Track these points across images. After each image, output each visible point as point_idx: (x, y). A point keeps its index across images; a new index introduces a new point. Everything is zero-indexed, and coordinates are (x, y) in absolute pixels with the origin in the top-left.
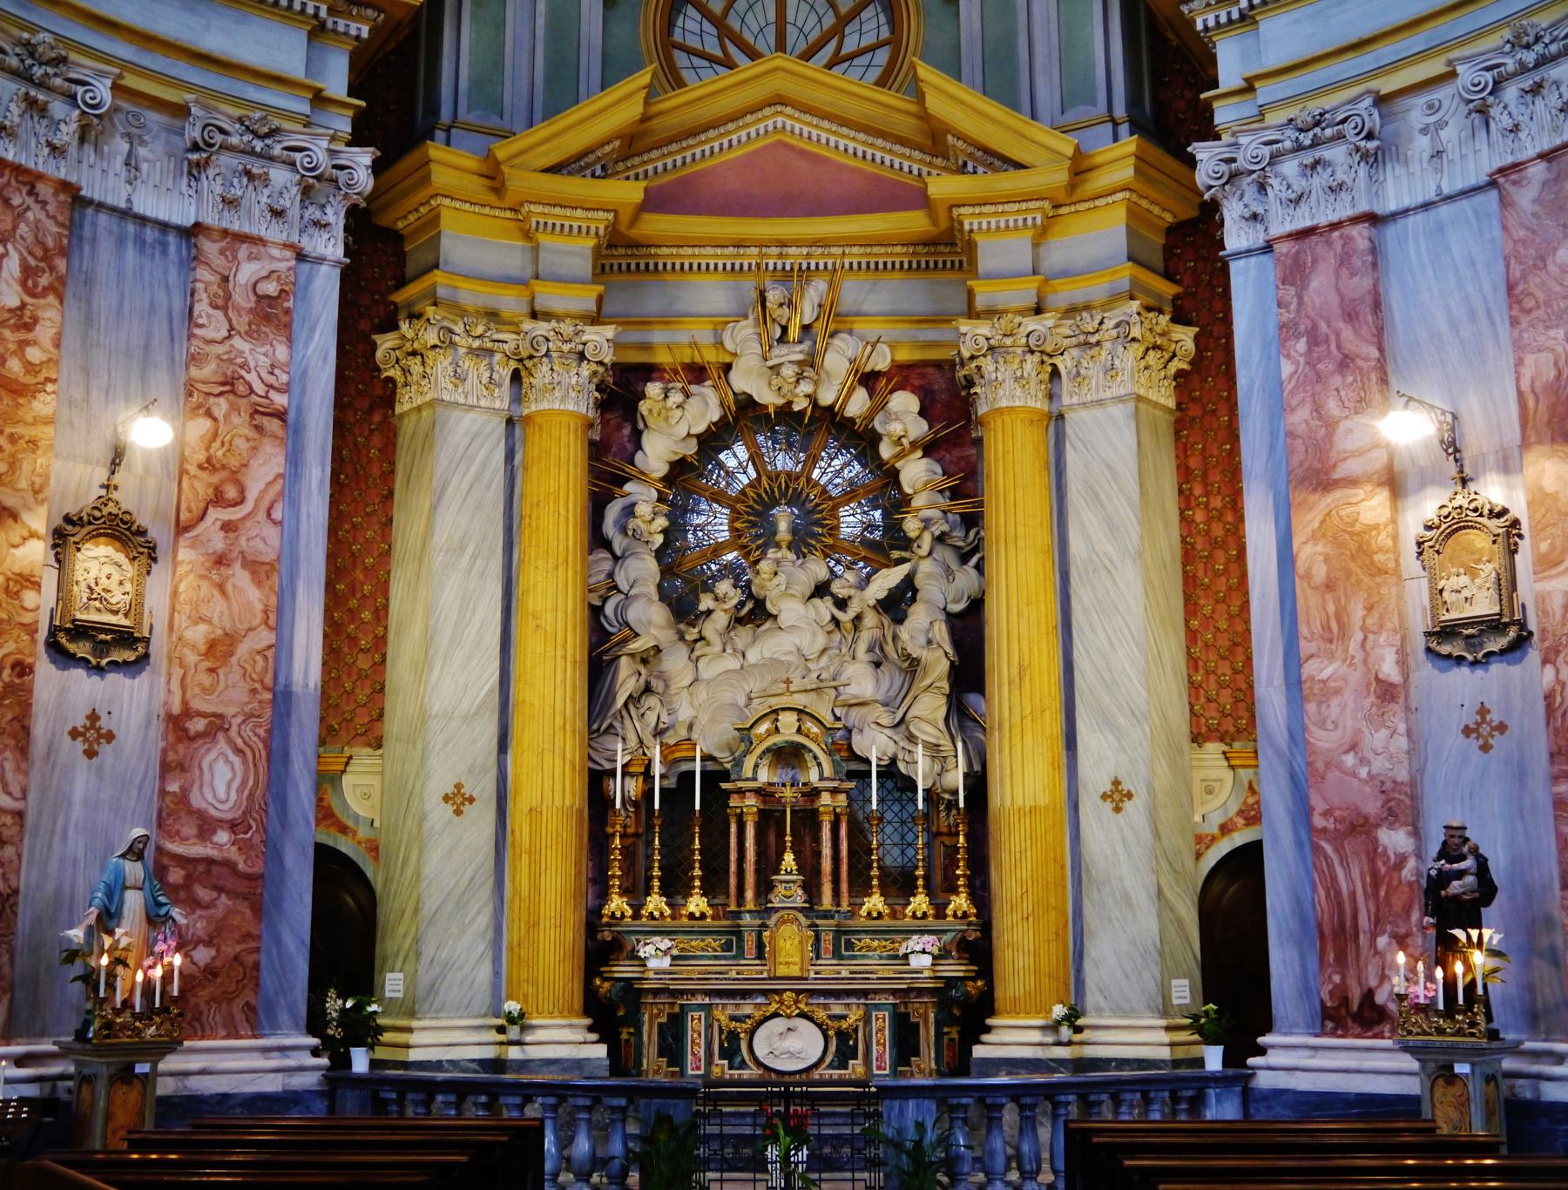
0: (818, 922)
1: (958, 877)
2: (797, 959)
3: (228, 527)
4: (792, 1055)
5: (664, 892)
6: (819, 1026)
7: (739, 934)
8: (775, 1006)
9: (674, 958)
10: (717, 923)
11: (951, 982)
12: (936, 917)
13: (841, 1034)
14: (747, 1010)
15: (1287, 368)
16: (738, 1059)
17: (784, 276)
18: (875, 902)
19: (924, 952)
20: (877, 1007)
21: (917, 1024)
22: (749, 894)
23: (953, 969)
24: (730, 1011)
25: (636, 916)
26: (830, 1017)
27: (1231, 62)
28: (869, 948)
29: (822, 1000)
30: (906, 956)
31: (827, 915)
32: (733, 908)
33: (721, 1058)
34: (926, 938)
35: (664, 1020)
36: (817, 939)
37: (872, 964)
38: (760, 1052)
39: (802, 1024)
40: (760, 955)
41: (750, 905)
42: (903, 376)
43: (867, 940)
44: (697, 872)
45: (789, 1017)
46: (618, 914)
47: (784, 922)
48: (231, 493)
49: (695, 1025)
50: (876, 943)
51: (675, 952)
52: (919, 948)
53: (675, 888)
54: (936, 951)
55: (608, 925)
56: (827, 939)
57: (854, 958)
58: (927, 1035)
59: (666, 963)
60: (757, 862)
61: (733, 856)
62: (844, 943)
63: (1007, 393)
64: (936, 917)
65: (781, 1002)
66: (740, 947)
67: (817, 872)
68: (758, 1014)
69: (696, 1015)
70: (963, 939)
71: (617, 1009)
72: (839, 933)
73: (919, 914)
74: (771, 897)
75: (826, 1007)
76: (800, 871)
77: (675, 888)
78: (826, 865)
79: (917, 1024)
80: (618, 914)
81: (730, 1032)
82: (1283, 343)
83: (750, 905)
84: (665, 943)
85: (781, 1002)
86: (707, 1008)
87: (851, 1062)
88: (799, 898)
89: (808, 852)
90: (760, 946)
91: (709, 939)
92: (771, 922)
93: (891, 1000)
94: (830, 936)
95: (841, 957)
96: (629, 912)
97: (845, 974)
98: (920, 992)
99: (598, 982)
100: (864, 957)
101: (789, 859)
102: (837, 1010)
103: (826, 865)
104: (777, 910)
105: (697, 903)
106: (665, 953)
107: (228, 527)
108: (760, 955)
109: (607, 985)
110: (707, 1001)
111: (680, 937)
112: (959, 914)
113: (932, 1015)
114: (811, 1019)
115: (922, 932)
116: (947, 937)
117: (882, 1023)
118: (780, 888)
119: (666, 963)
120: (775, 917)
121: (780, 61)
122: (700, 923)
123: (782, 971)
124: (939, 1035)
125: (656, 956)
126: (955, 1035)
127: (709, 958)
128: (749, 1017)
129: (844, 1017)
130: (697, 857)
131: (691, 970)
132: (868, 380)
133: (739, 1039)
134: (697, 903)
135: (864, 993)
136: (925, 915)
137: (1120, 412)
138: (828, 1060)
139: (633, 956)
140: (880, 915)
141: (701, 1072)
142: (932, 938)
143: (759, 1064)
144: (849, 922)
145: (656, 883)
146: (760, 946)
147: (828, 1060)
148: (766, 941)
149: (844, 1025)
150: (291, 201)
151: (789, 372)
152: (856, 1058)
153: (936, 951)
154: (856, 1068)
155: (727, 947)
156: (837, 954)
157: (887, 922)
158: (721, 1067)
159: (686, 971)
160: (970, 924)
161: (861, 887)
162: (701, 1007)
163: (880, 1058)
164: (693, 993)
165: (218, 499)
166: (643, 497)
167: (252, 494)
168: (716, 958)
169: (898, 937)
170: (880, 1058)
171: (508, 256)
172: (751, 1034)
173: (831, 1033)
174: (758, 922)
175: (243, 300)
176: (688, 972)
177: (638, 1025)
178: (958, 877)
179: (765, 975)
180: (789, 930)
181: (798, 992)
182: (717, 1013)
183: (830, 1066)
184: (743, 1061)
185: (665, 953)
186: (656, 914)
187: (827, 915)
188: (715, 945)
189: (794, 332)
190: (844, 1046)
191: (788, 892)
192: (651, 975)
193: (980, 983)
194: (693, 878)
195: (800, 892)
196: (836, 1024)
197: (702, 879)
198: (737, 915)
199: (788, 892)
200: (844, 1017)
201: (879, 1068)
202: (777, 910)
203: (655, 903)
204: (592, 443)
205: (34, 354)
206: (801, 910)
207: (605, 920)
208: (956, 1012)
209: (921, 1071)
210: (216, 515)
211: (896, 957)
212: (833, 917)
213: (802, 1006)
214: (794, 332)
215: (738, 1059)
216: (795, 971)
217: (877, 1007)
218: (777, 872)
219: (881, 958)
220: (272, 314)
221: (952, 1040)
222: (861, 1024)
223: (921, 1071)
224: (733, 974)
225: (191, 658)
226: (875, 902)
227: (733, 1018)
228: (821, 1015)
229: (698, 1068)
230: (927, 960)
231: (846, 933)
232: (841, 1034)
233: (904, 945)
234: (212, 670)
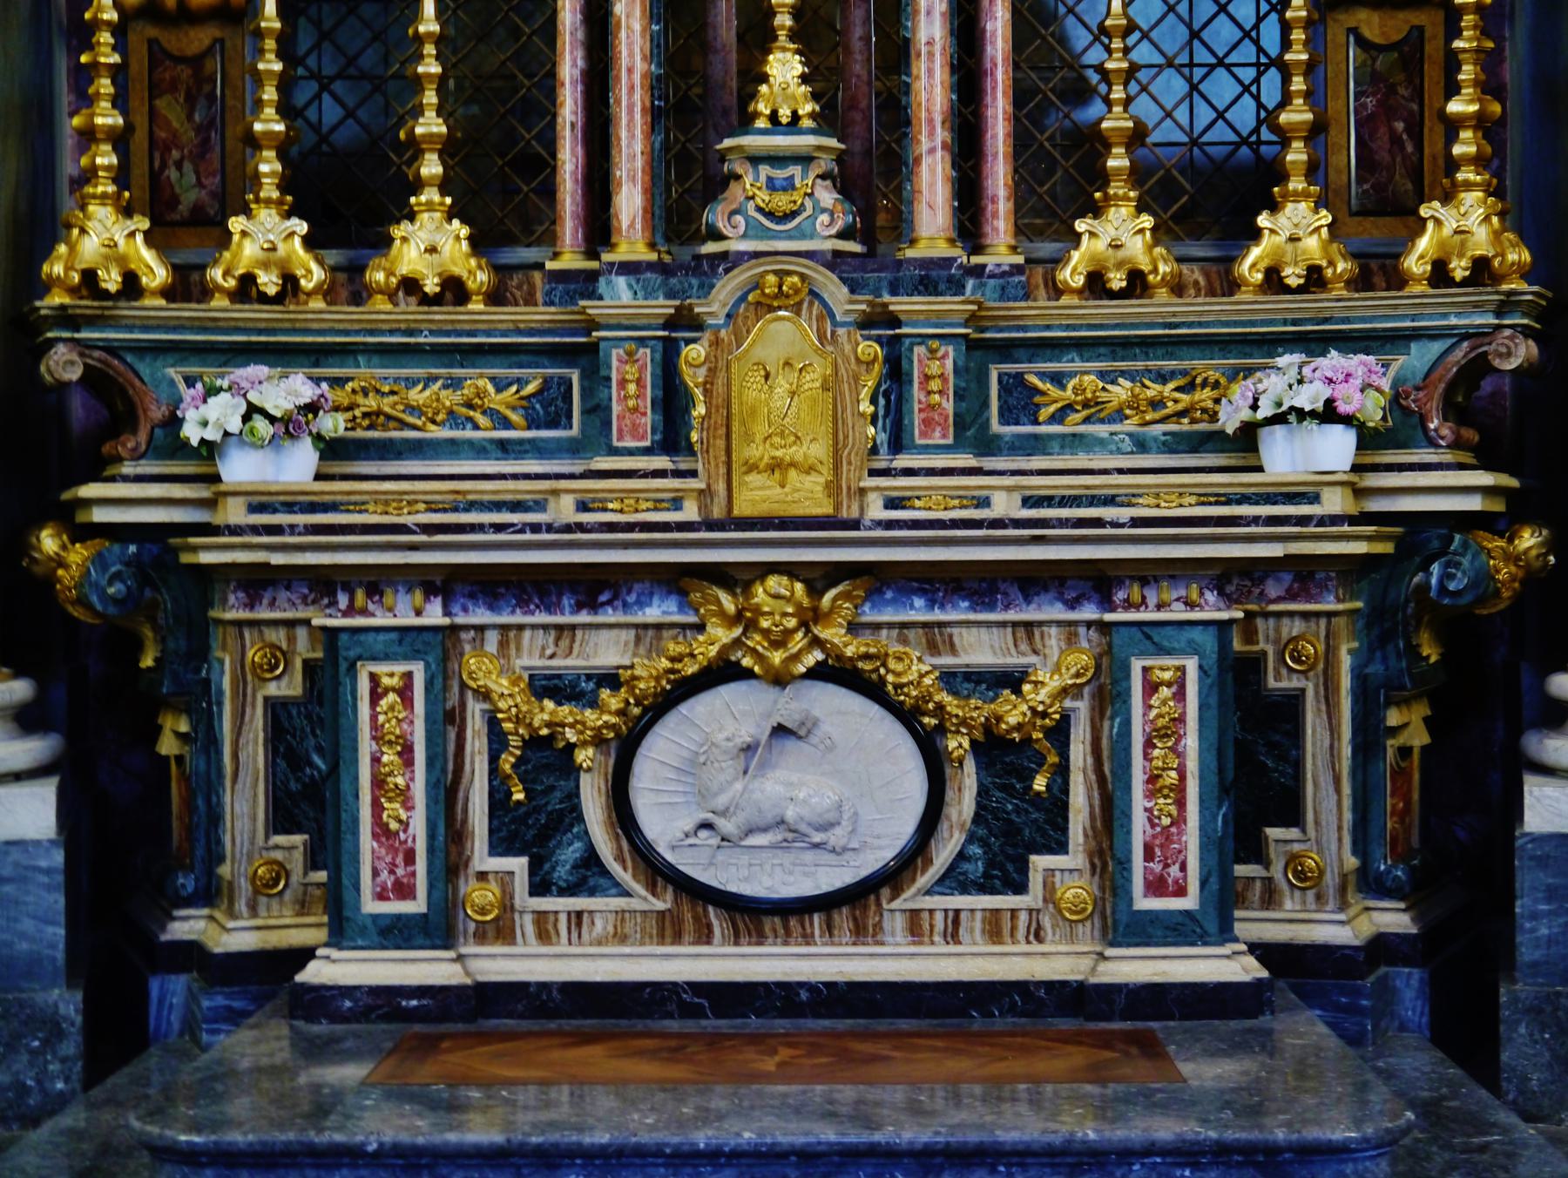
0: (901, 304)
1: (1452, 127)
2: (818, 450)
4: (793, 836)
5: (301, 195)
6: (907, 716)
7: (588, 357)
8: (721, 635)
9: (331, 449)
10: (505, 315)
11: (1421, 535)
12: (1361, 282)
13: (993, 748)
14: (605, 649)
16: (570, 853)
18: (1119, 233)
19: (1329, 414)
20: (1151, 636)
21: (1292, 704)
22: (629, 202)
23: (1449, 486)
24: (533, 655)
25: (187, 284)
26: (949, 679)
28: (1094, 409)
29: (918, 611)
30: (1247, 438)
31: (932, 278)
32: (571, 260)
33: (500, 846)
34: (1334, 361)
35: (290, 687)
36: (896, 372)
37: (1108, 467)
38: (663, 821)
39: (836, 707)
40: (672, 438)
41: (632, 243)
43: (1085, 377)
44: (431, 125)
45: (780, 680)
46: (111, 280)
47: (765, 307)
49: (386, 715)
50: (1121, 391)
51: (332, 424)
52: (1309, 397)
53: (349, 203)
54: (1372, 409)
55: (64, 318)
56: (935, 372)
57: (1035, 445)
58: (1325, 746)
59: (297, 466)
60: (656, 85)
61: (570, 66)
62: (1001, 385)
64: (1361, 282)
65: (746, 620)
66: (598, 412)
67: (896, 112)
68: (649, 671)
69: (390, 672)
70: (1478, 367)
71: (138, 648)
72: (979, 349)
73: (1293, 276)
74: (716, 215)
75: (935, 637)
76: (827, 120)
77: (349, 203)
78: (931, 88)
79: (1297, 697)
80: (111, 280)
81: (534, 743)
83: (632, 243)
84: (286, 391)
85: (746, 620)
86: (440, 647)
87: (1040, 862)
88: (825, 216)
89: (860, 66)
90: (672, 400)
91: (478, 380)
92: (715, 304)
93: (1213, 610)
94: (947, 360)
95: (988, 445)
96: (155, 272)
97: (1004, 505)
98: (1305, 574)
99: (48, 542)
100: (1075, 442)
101: (784, 67)
102: (981, 648)
103: (931, 88)
104: (729, 261)
105: (429, 243)
106: (289, 426)
108: (672, 438)
109: (78, 555)
110: (434, 615)
111: (364, 372)
112: (1459, 269)
113: (1346, 662)
114: (873, 690)
115: (1314, 343)
116: (1419, 357)
117: (1173, 702)
118: (752, 184)
119: (297, 466)
120: (726, 288)
122: (440, 314)
123: (756, 495)
124: (1369, 736)
125: (252, 439)
126: (1418, 738)
127: (479, 450)
128: (611, 680)
129: (1013, 680)
130: (430, 67)
131: (396, 493)
133: (571, 771)
134: (429, 243)
135: (1099, 581)
136: (1315, 278)
138: (944, 852)
139: (168, 439)
140: (1137, 283)
141: (416, 906)
142: (1357, 363)
143: (656, 870)
144: (1020, 308)
145: (269, 166)
146: (672, 400)
147: (944, 852)
148: (693, 378)
149: (1013, 712)
152: (1061, 847)
153: (1372, 409)
154: (1063, 871)
155: (548, 408)
156: (970, 431)
157: (1161, 304)
158: (496, 871)
159: (380, 492)
160: (1505, 306)
161: (1062, 184)
162: (409, 640)
163: (1163, 844)
164: (376, 582)
168: (505, 449)
169: (1207, 366)
170: (1163, 844)
172: (625, 748)
173: (956, 743)
174: (663, 306)
176: (385, 501)
177: (199, 701)
178: (1452, 127)
179: (690, 512)
180: (781, 335)
181: (819, 578)
182: (480, 667)
183: (954, 880)
184: (590, 859)
185: (289, 426)
186: (269, 282)
187: (932, 278)
188: (499, 400)
190: (1009, 806)
191: (783, 203)
192: (234, 513)
193: (1528, 540)
194: (415, 149)
195: (827, 196)
196: (976, 709)
197: (448, 149)
198: (584, 284)
199: (783, 203)
200: (1013, 680)
201: (1157, 886)
202: (729, 261)
203: (266, 238)
206: (835, 261)
207: (57, 298)
208: (1430, 651)
209: (1305, 879)
211: (1213, 440)
212: (957, 287)
213: (833, 634)
215: (570, 853)
216: (807, 494)
217: (1151, 636)
218: (745, 122)
219: (1141, 445)
221: (1405, 752)
222: (1081, 708)
223: (1305, 879)
224: (564, 510)
226: (1119, 233)
227: (548, 687)
228: (914, 670)
229: (404, 890)
230: (1335, 449)
231: (1005, 350)
232: (993, 748)
233: (1240, 392)
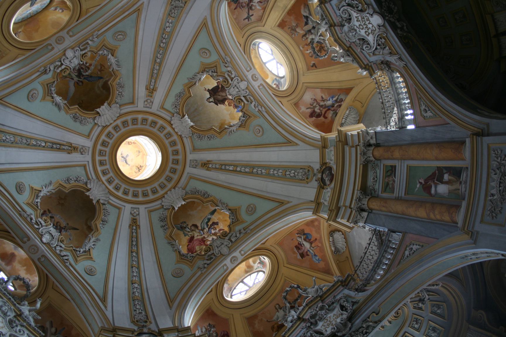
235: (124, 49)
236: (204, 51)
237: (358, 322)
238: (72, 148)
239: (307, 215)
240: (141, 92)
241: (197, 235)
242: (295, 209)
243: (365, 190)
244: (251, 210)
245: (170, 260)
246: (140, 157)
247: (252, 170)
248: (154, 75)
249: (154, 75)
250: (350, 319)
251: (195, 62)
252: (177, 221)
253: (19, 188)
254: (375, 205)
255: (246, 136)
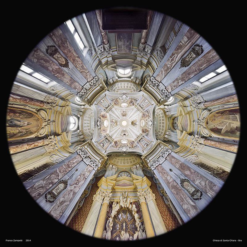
3: (75, 187)
15: (161, 175)
17: (125, 192)
27: (148, 161)
42: (135, 203)
48: (77, 184)
63: (142, 201)
82: (159, 174)
107: (75, 187)
121: (124, 176)
132: (131, 203)
137: (151, 201)
150: (95, 166)
151: (125, 201)
165: (76, 184)
166: (111, 220)
167: (79, 185)
171: (106, 188)
175: (88, 170)
189: (125, 198)
204: (107, 211)
205: (72, 166)
210: (75, 185)
214: (125, 198)
220: (90, 172)
225: (58, 203)
234: (59, 206)
235: (135, 128)
236: (130, 136)
237: (97, 125)
238: (130, 118)
239: (108, 132)
240: (130, 128)
241: (113, 123)
242: (109, 132)
243: (107, 139)
244: (112, 129)
245: (114, 118)
246: (124, 123)
247: (116, 132)
248: (131, 130)
249: (131, 130)
250: (97, 125)
251: (130, 134)
252: (116, 122)
253: (130, 111)
254: (105, 138)
255: (119, 134)
